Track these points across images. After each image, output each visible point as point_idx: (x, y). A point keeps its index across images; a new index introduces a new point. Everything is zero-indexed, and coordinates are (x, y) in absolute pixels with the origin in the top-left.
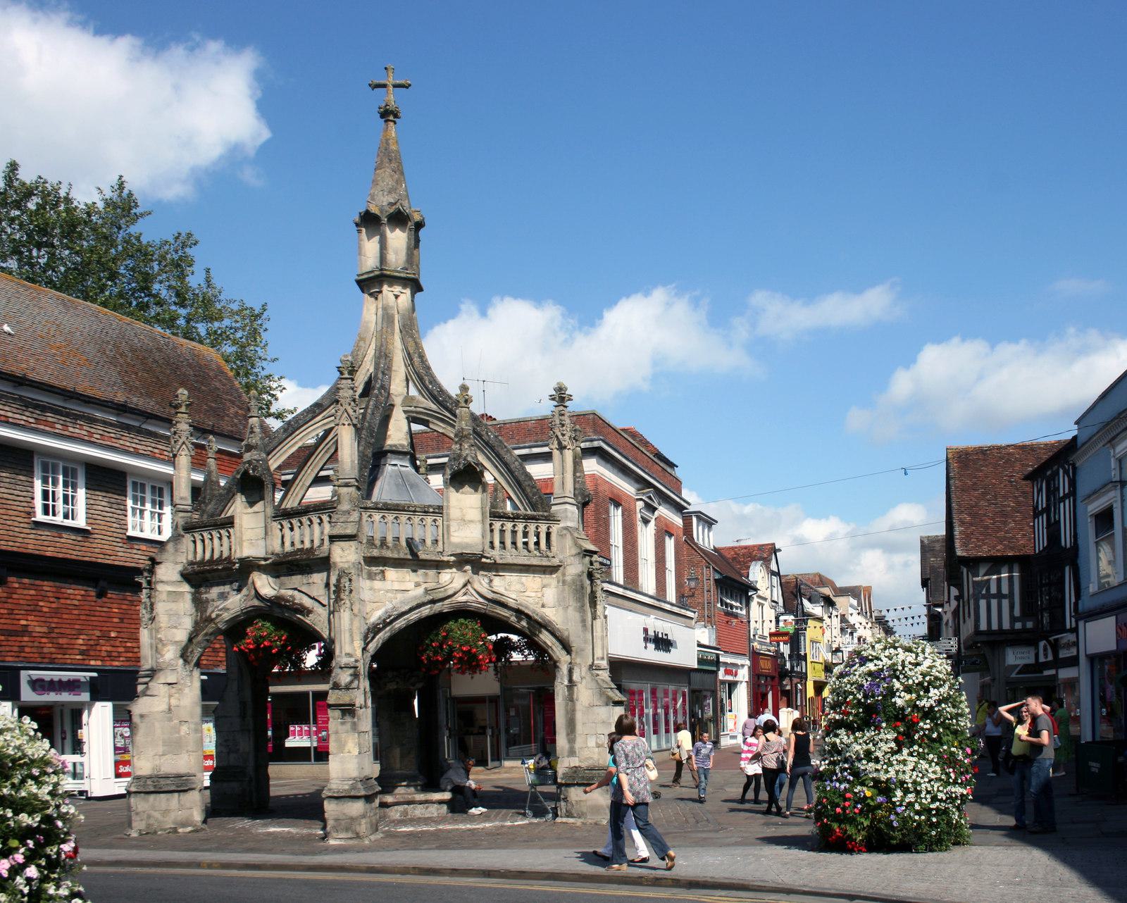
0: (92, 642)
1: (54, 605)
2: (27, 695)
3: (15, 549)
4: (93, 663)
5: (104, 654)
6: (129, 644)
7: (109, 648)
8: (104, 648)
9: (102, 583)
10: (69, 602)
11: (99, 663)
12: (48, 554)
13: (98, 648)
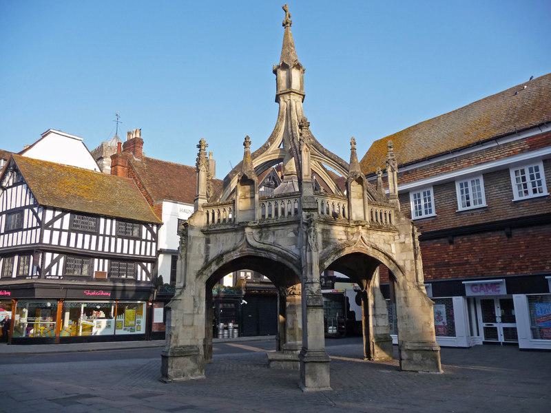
0: (507, 262)
1: (481, 247)
2: (469, 293)
3: (451, 227)
4: (509, 273)
5: (516, 268)
6: (534, 260)
7: (519, 264)
8: (515, 265)
9: (508, 230)
10: (490, 244)
11: (513, 273)
12: (467, 225)
13: (512, 265)
